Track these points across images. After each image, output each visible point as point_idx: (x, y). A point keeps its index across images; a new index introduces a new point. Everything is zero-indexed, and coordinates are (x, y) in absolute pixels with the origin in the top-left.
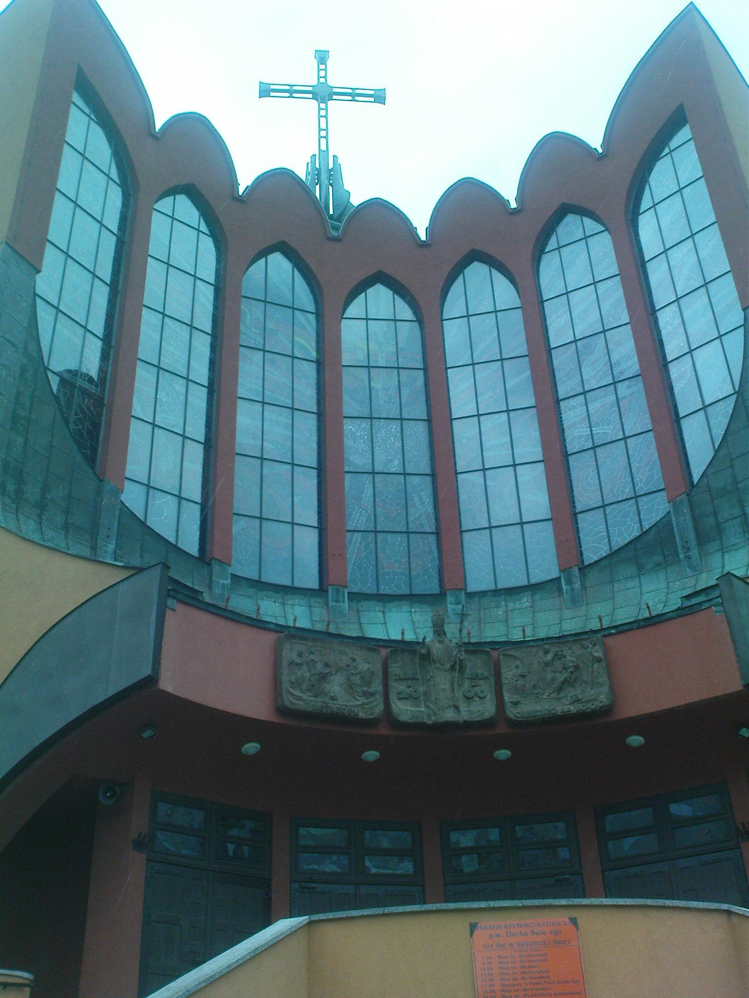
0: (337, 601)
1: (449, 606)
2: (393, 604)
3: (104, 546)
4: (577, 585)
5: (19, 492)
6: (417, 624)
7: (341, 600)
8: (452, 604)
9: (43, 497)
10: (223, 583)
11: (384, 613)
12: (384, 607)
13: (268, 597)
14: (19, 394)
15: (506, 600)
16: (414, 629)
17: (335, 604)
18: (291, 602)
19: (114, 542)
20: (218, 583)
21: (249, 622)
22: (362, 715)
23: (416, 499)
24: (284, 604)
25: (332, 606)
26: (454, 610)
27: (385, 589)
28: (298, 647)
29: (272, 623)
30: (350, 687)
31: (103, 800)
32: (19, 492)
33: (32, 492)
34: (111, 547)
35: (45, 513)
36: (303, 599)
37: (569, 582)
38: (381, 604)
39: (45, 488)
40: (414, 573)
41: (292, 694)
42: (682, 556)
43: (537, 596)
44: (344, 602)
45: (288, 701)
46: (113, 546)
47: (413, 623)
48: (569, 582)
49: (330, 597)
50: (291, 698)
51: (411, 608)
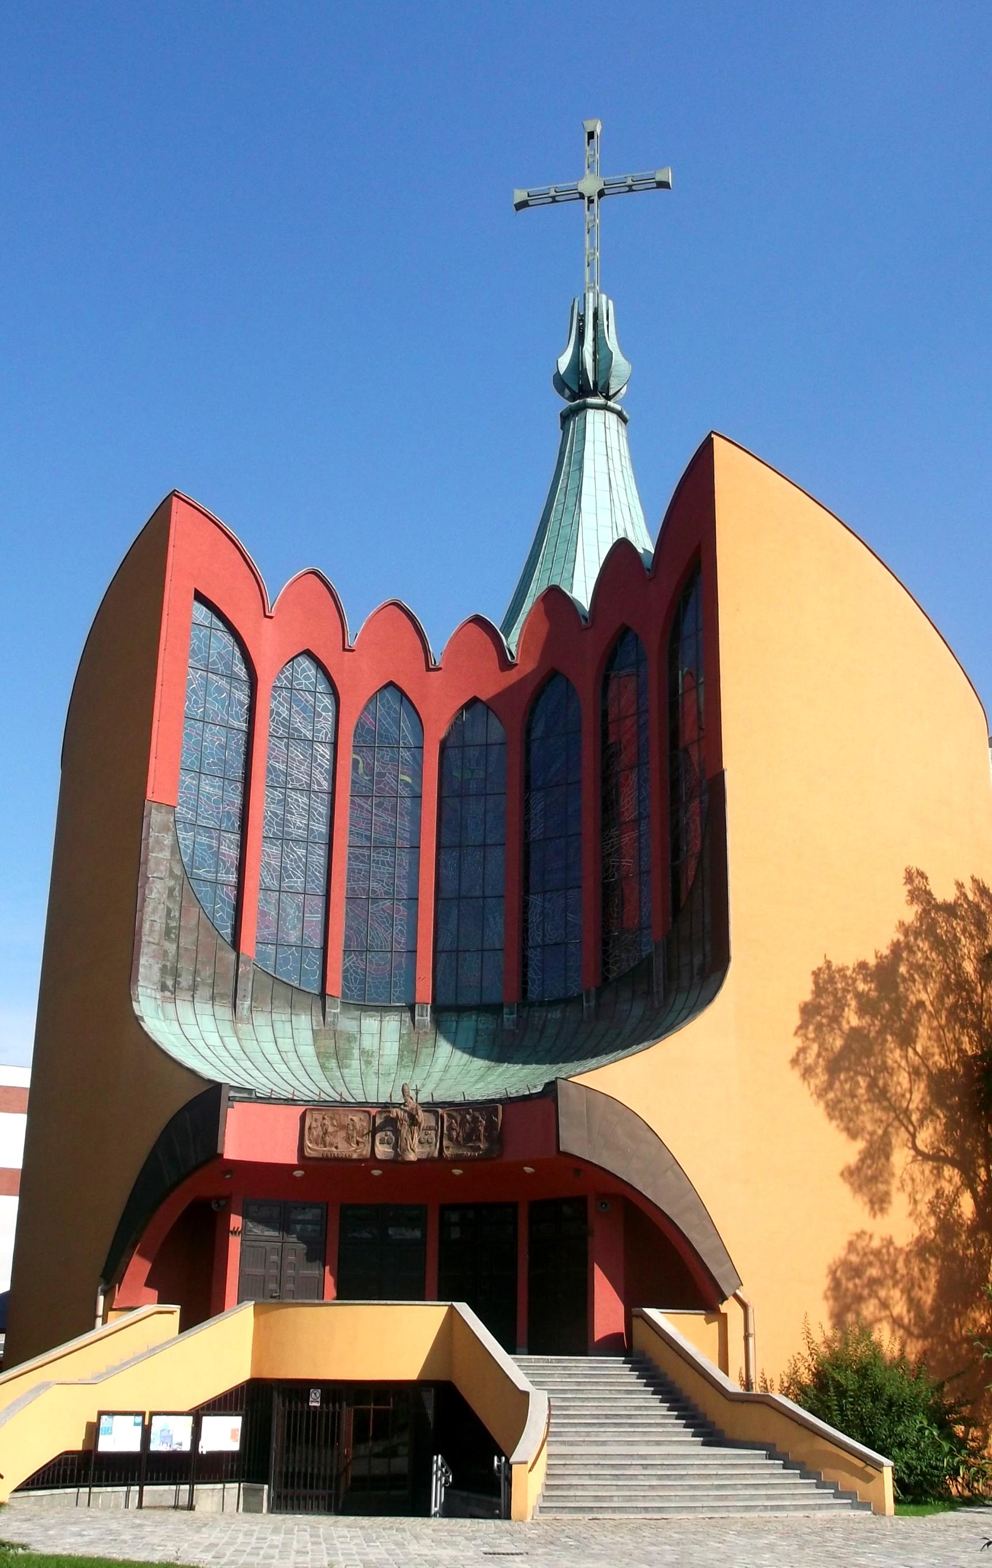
0: (422, 1016)
1: (505, 1016)
2: (465, 1014)
3: (242, 1004)
4: (593, 1003)
5: (176, 983)
6: (480, 1032)
7: (425, 1015)
8: (507, 1014)
9: (194, 981)
10: (334, 1013)
11: (457, 1022)
12: (458, 1016)
13: (372, 1017)
14: (169, 911)
15: (547, 1011)
16: (476, 1037)
17: (420, 1018)
18: (387, 1018)
19: (249, 999)
20: (331, 1012)
21: (286, 1102)
22: (355, 1156)
23: (491, 919)
24: (381, 1021)
25: (418, 1020)
26: (508, 1019)
27: (463, 1001)
28: (317, 1115)
29: (302, 1100)
30: (348, 1139)
31: (214, 1206)
32: (176, 983)
33: (185, 980)
34: (247, 1003)
35: (197, 992)
36: (397, 1015)
37: (588, 1001)
38: (456, 1014)
39: (196, 972)
40: (485, 985)
41: (309, 1148)
42: (655, 990)
43: (568, 1009)
44: (427, 1015)
45: (308, 1153)
46: (249, 1003)
47: (477, 1030)
48: (588, 1001)
49: (416, 1013)
50: (309, 1150)
51: (478, 1017)
